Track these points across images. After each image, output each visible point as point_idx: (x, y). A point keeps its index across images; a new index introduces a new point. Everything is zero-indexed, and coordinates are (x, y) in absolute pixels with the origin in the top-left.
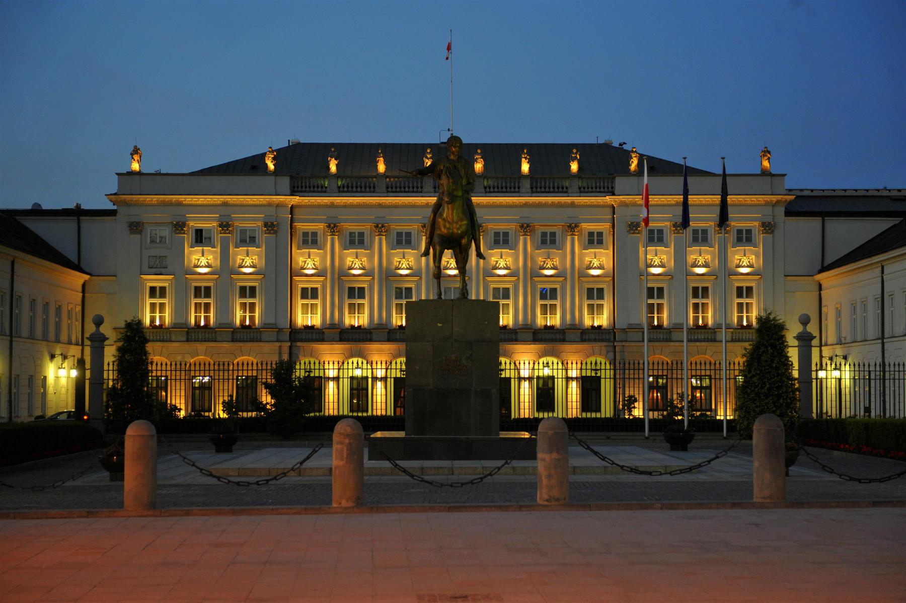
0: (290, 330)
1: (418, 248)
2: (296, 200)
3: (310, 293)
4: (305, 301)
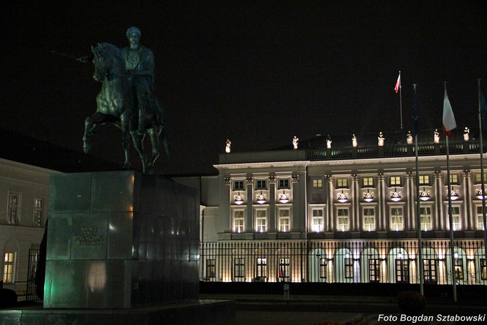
0: (307, 233)
1: (376, 187)
2: (308, 163)
4: (316, 218)
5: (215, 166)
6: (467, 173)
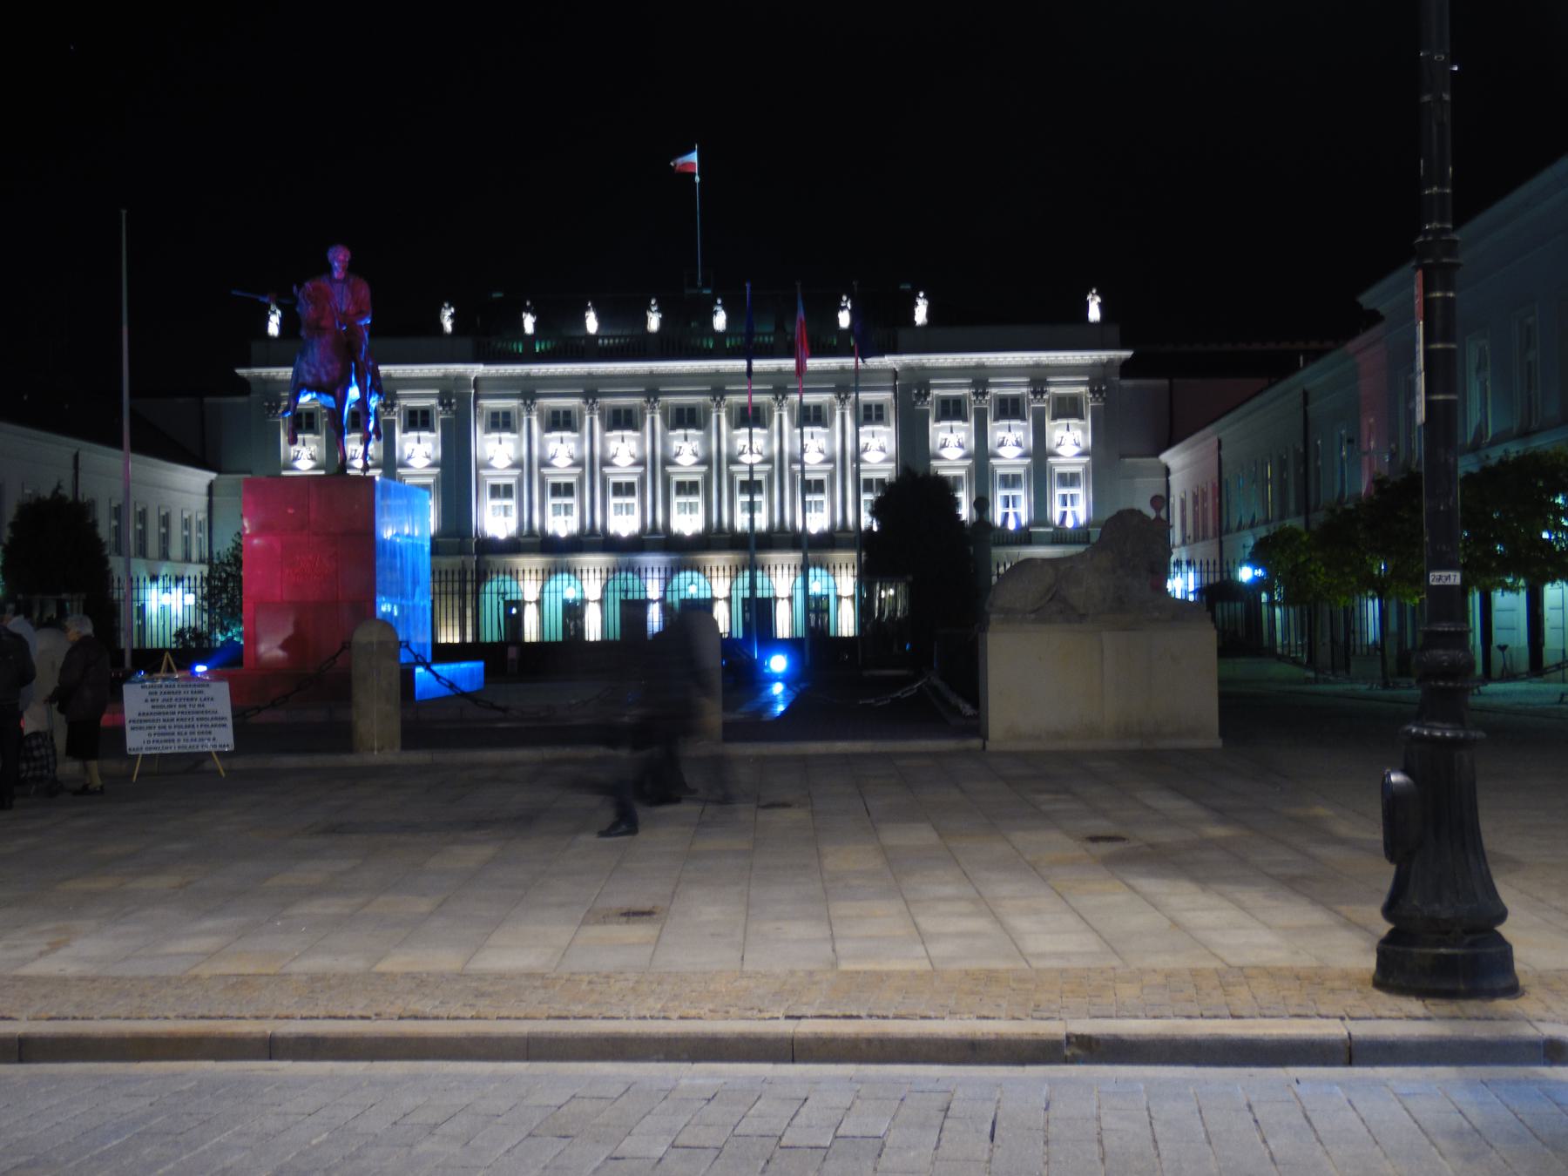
0: (475, 540)
2: (478, 370)
3: (500, 491)
5: (241, 372)
6: (843, 401)
